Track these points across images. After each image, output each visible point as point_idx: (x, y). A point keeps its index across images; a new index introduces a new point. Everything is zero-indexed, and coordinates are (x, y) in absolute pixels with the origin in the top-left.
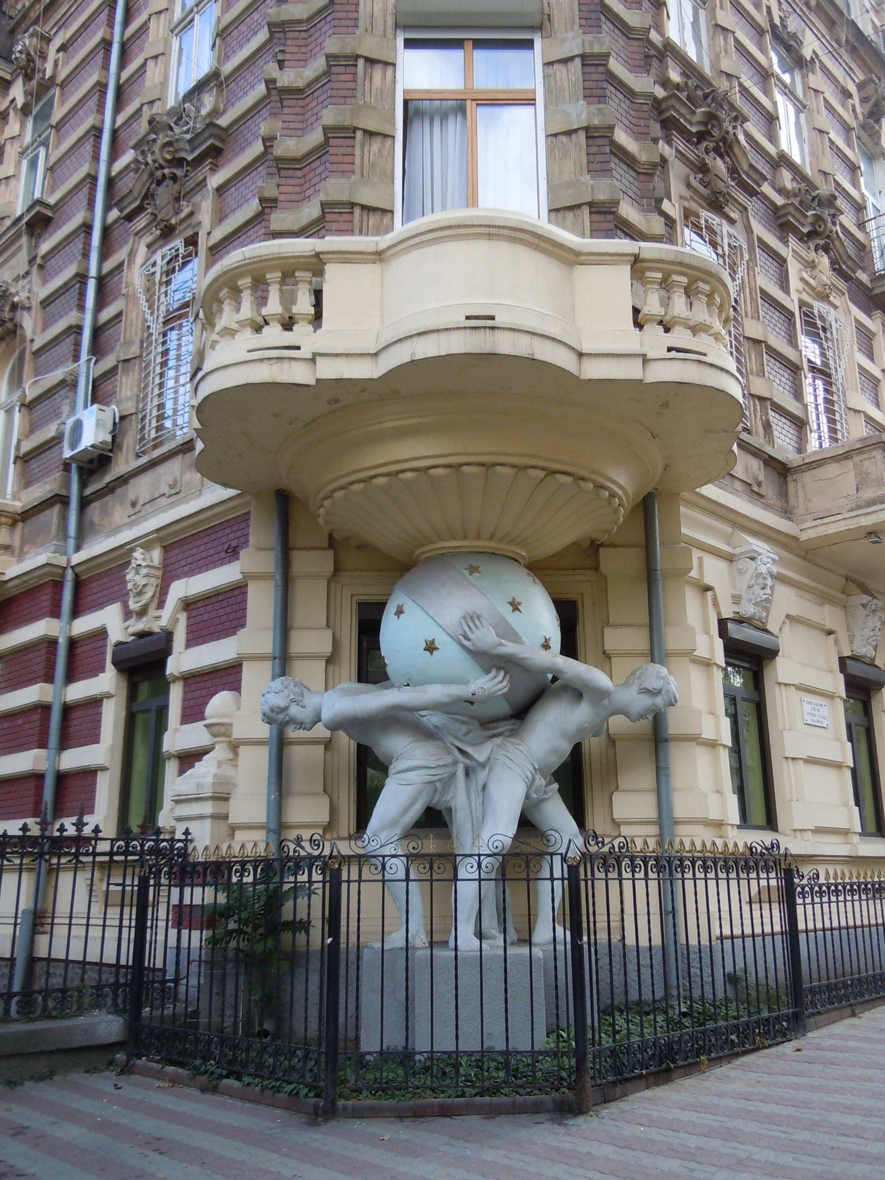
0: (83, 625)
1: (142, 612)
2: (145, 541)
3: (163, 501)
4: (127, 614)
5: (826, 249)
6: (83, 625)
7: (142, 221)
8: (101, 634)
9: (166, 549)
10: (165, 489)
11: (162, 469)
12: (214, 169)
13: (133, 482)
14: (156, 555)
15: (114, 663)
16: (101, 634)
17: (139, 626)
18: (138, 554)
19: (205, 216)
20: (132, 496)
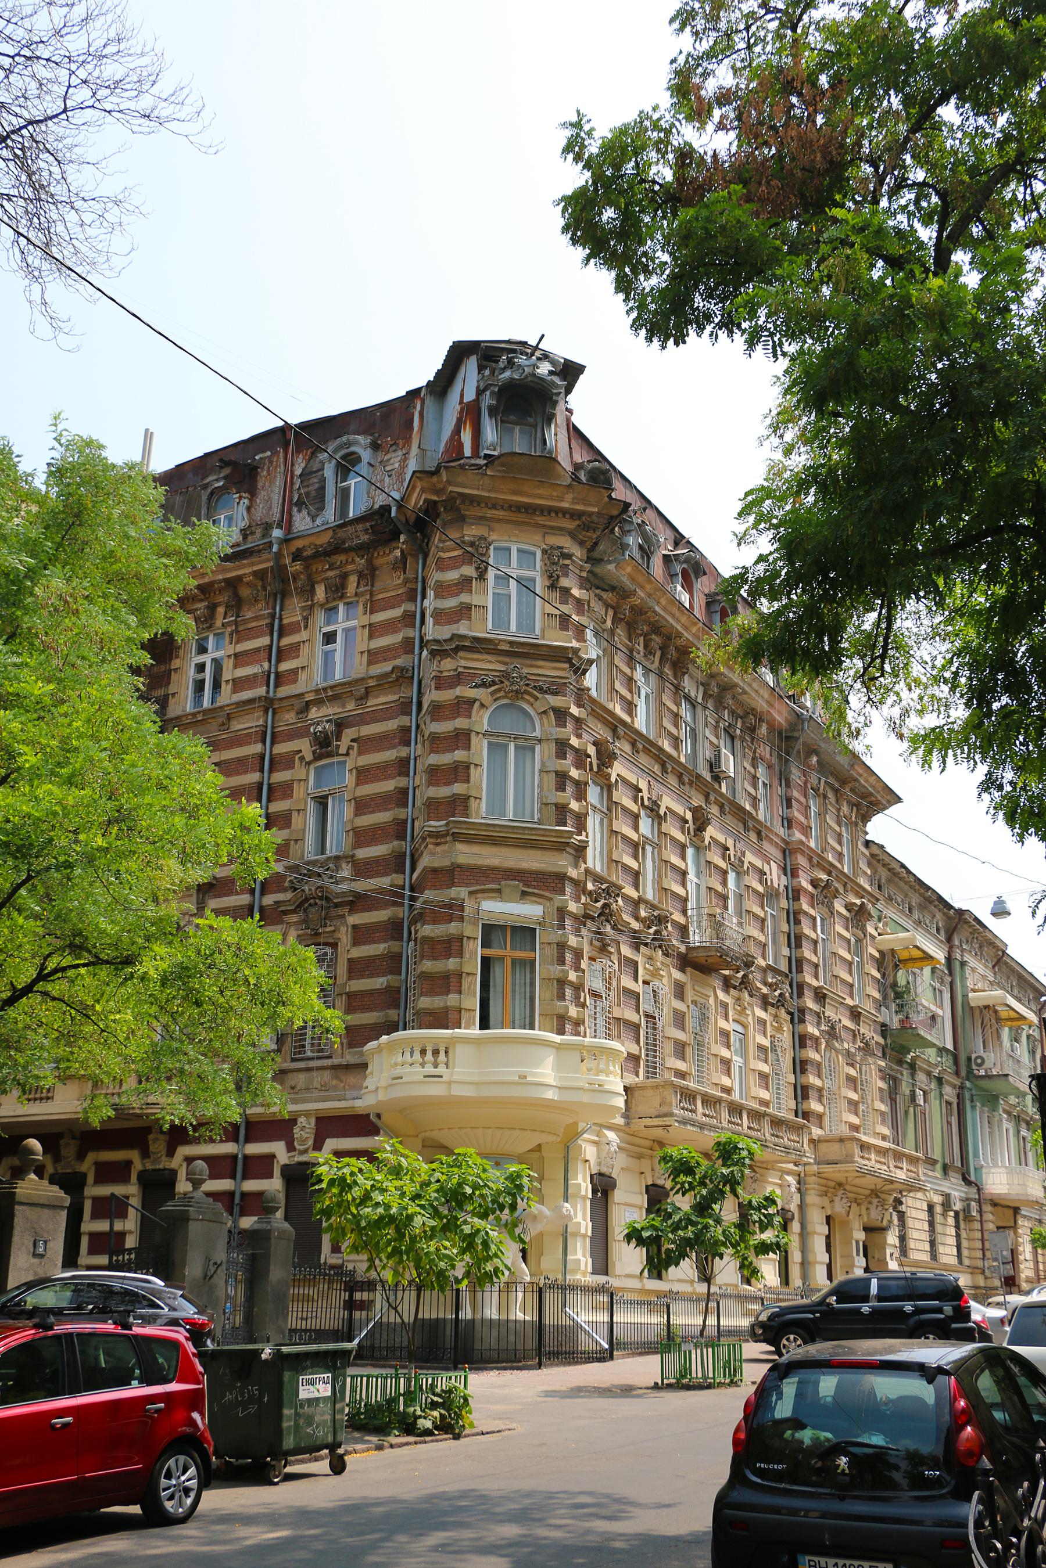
0: (254, 1149)
1: (305, 1151)
2: (307, 1114)
3: (317, 1094)
4: (290, 1148)
5: (660, 947)
6: (254, 1149)
7: (293, 918)
8: (272, 1157)
9: (318, 1119)
10: (316, 1084)
11: (315, 1074)
12: (351, 912)
13: (290, 1075)
14: (313, 1121)
15: (282, 1174)
16: (272, 1157)
17: (303, 1158)
18: (302, 1120)
19: (345, 937)
20: (293, 1083)
